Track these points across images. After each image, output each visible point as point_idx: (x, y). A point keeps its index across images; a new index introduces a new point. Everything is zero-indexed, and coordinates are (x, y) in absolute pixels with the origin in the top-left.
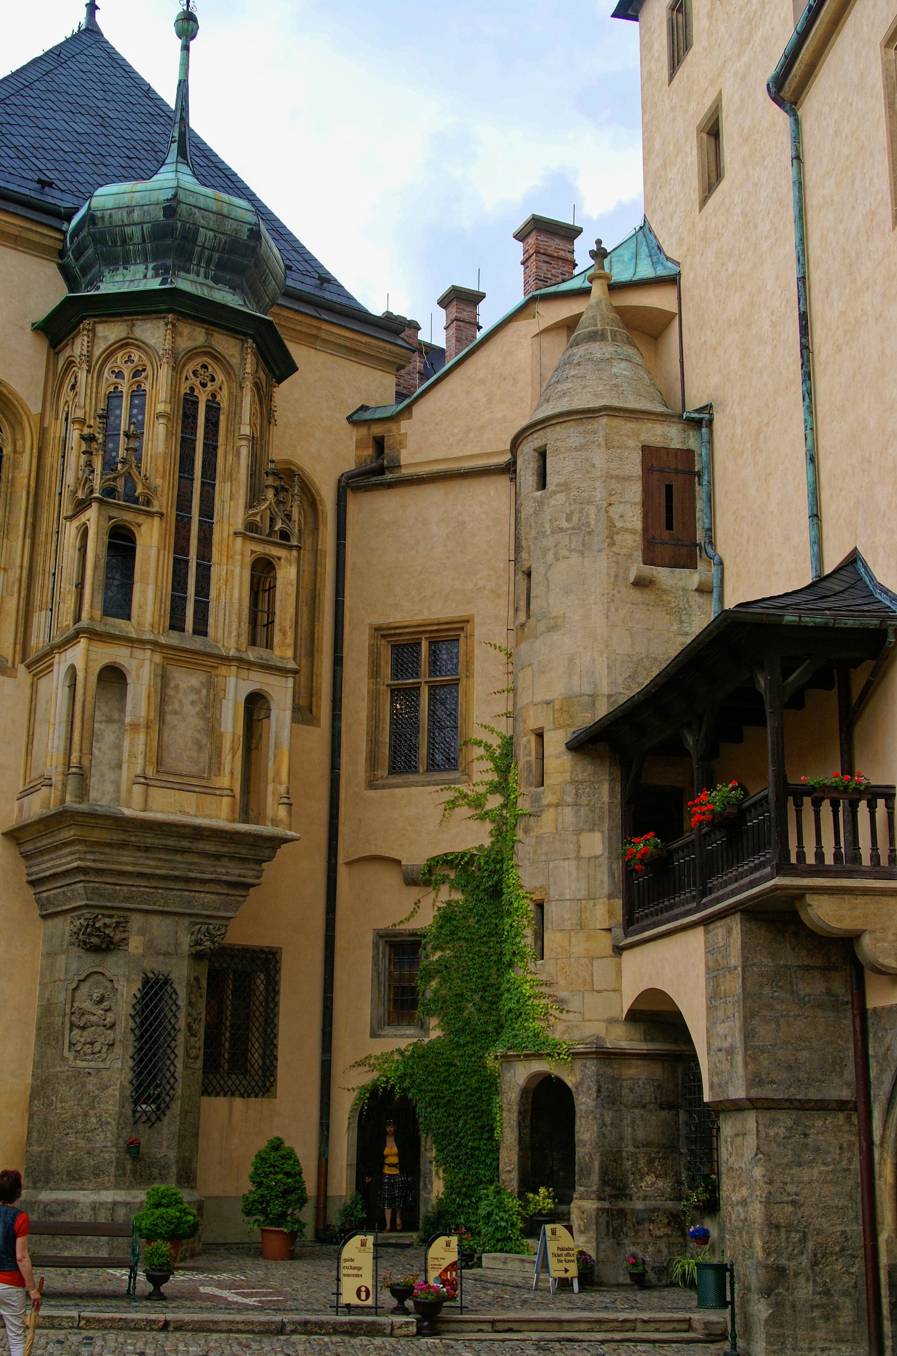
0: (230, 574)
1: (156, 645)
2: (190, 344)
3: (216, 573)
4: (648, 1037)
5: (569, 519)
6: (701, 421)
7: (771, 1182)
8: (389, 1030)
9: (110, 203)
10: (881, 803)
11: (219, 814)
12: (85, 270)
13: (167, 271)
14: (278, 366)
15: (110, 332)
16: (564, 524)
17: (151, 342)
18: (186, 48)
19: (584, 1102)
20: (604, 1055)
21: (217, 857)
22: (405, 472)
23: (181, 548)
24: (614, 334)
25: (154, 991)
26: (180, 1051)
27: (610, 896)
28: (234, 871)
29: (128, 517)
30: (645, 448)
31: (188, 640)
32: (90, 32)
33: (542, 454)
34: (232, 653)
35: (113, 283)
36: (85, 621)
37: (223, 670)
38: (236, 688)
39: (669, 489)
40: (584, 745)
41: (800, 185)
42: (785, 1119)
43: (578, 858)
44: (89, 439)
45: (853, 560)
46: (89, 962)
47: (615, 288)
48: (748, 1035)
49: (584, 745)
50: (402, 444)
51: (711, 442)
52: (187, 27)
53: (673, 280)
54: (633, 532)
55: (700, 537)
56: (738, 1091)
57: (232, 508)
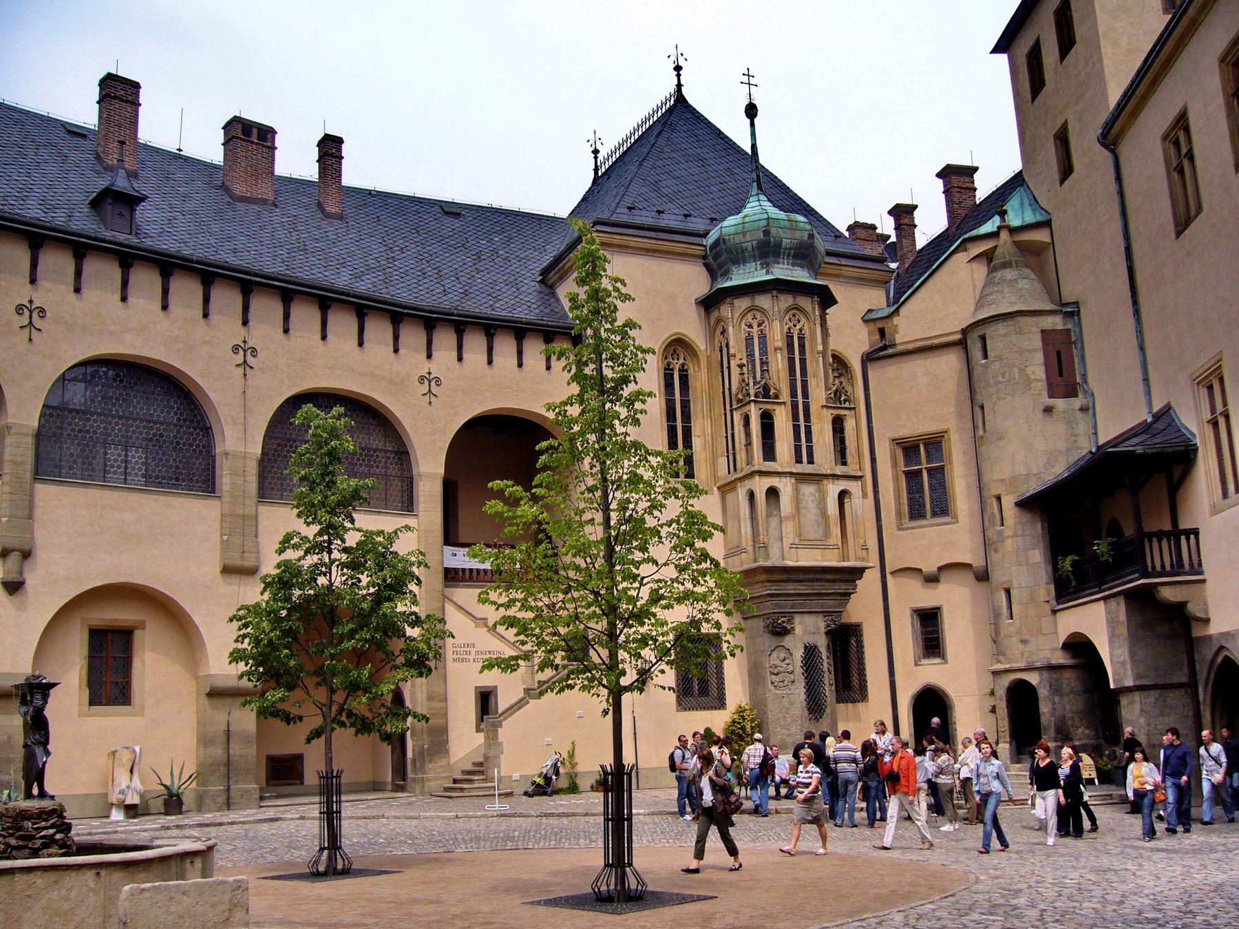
0: (822, 428)
1: (791, 474)
2: (787, 305)
3: (815, 429)
4: (1073, 657)
5: (1003, 376)
7: (1149, 725)
8: (924, 661)
9: (732, 230)
10: (1192, 537)
11: (832, 561)
12: (720, 266)
13: (768, 265)
14: (826, 299)
15: (742, 303)
16: (1001, 379)
17: (765, 307)
18: (752, 125)
19: (1043, 693)
20: (1052, 668)
21: (834, 581)
22: (900, 348)
23: (795, 417)
24: (1017, 262)
25: (810, 651)
26: (826, 682)
27: (1047, 583)
28: (842, 588)
29: (769, 407)
30: (1042, 331)
31: (805, 468)
32: (680, 99)
33: (983, 339)
34: (829, 472)
35: (742, 276)
36: (756, 468)
37: (825, 482)
38: (833, 489)
39: (1059, 354)
40: (1025, 504)
41: (1121, 194)
42: (1154, 694)
43: (1027, 564)
44: (741, 366)
45: (1167, 409)
46: (775, 641)
47: (1013, 231)
48: (1132, 655)
49: (1025, 504)
50: (896, 332)
51: (1080, 324)
52: (751, 111)
53: (1047, 224)
54: (1041, 380)
55: (1078, 379)
56: (1129, 683)
57: (818, 394)
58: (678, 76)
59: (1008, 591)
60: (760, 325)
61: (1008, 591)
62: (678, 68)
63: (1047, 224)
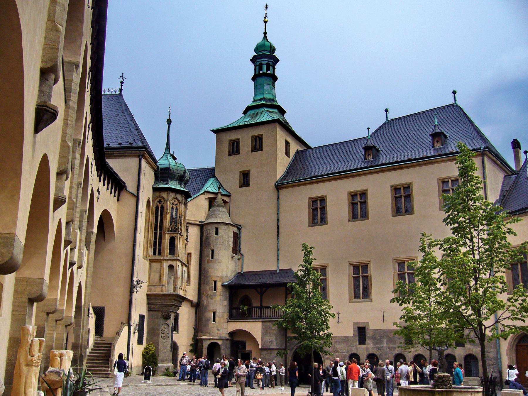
6: (239, 229)
18: (169, 127)
19: (223, 347)
53: (229, 196)
58: (122, 85)
59: (214, 314)
60: (176, 205)
61: (214, 314)
62: (122, 83)
63: (229, 196)
